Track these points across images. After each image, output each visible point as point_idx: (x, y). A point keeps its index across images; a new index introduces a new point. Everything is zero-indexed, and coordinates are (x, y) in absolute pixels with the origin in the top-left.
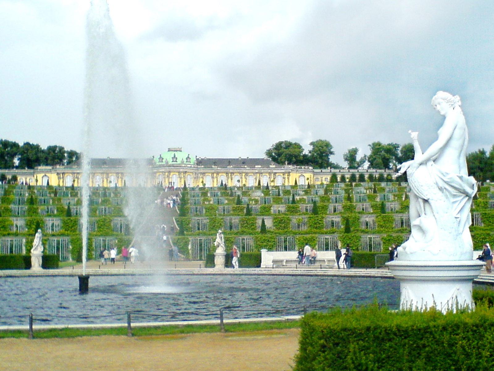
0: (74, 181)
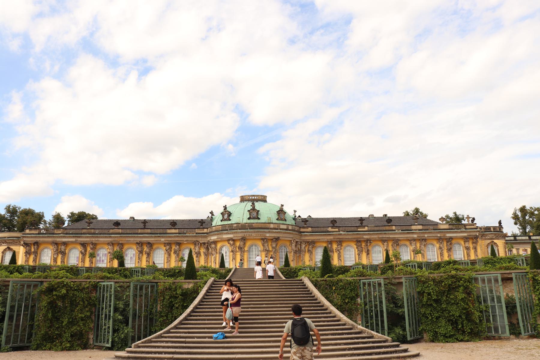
0: (55, 260)
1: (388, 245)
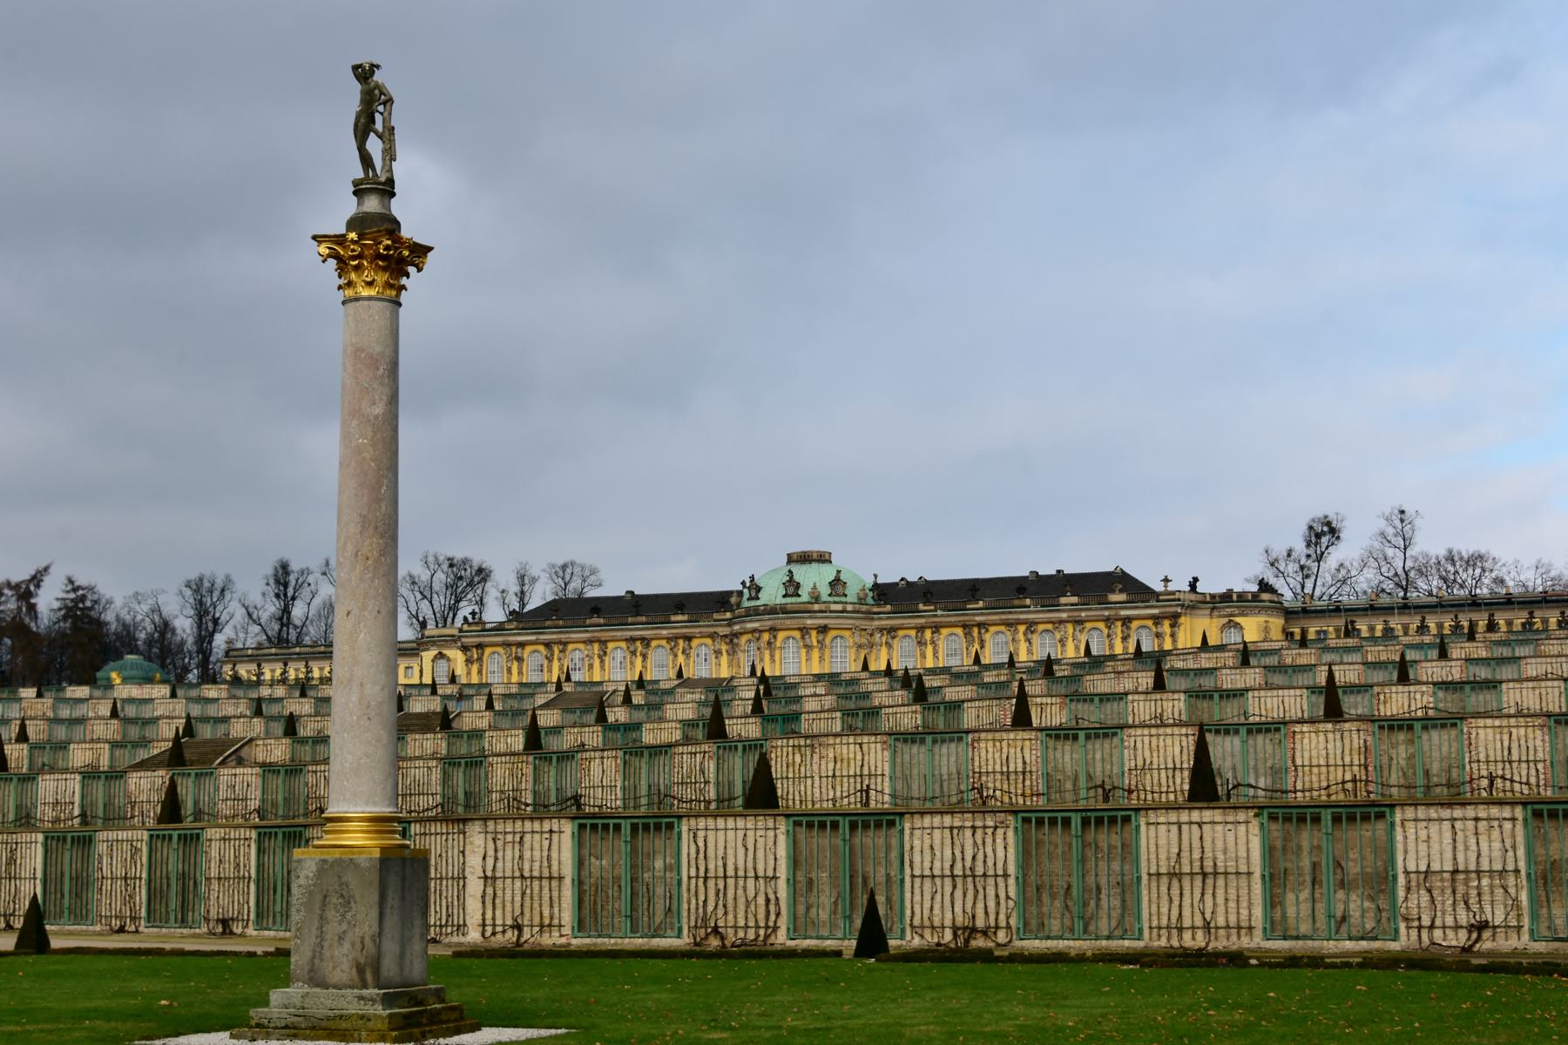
0: (509, 671)
1: (1016, 631)
